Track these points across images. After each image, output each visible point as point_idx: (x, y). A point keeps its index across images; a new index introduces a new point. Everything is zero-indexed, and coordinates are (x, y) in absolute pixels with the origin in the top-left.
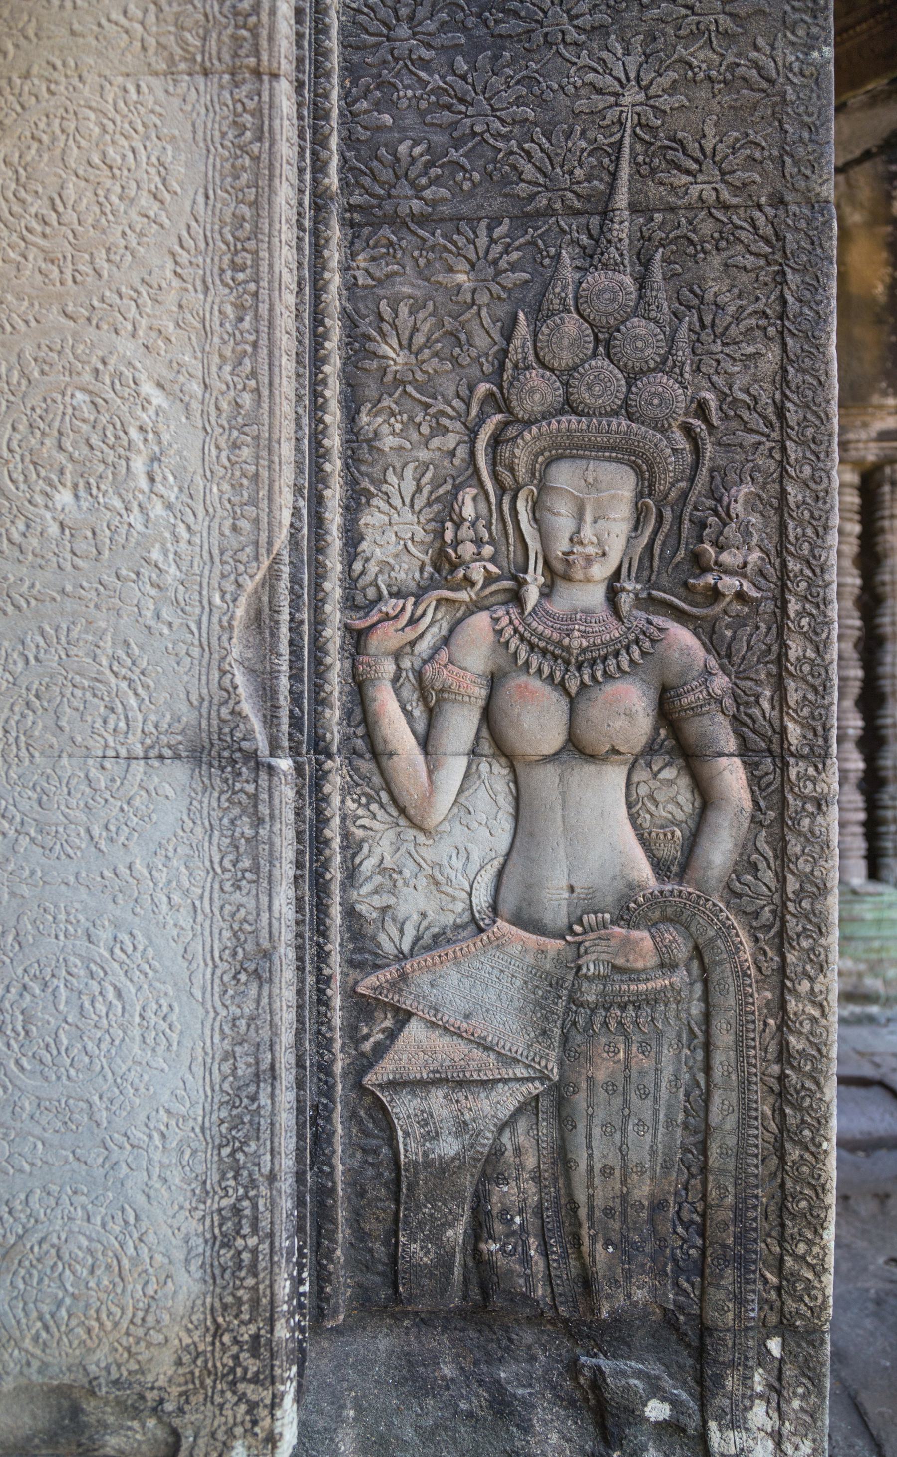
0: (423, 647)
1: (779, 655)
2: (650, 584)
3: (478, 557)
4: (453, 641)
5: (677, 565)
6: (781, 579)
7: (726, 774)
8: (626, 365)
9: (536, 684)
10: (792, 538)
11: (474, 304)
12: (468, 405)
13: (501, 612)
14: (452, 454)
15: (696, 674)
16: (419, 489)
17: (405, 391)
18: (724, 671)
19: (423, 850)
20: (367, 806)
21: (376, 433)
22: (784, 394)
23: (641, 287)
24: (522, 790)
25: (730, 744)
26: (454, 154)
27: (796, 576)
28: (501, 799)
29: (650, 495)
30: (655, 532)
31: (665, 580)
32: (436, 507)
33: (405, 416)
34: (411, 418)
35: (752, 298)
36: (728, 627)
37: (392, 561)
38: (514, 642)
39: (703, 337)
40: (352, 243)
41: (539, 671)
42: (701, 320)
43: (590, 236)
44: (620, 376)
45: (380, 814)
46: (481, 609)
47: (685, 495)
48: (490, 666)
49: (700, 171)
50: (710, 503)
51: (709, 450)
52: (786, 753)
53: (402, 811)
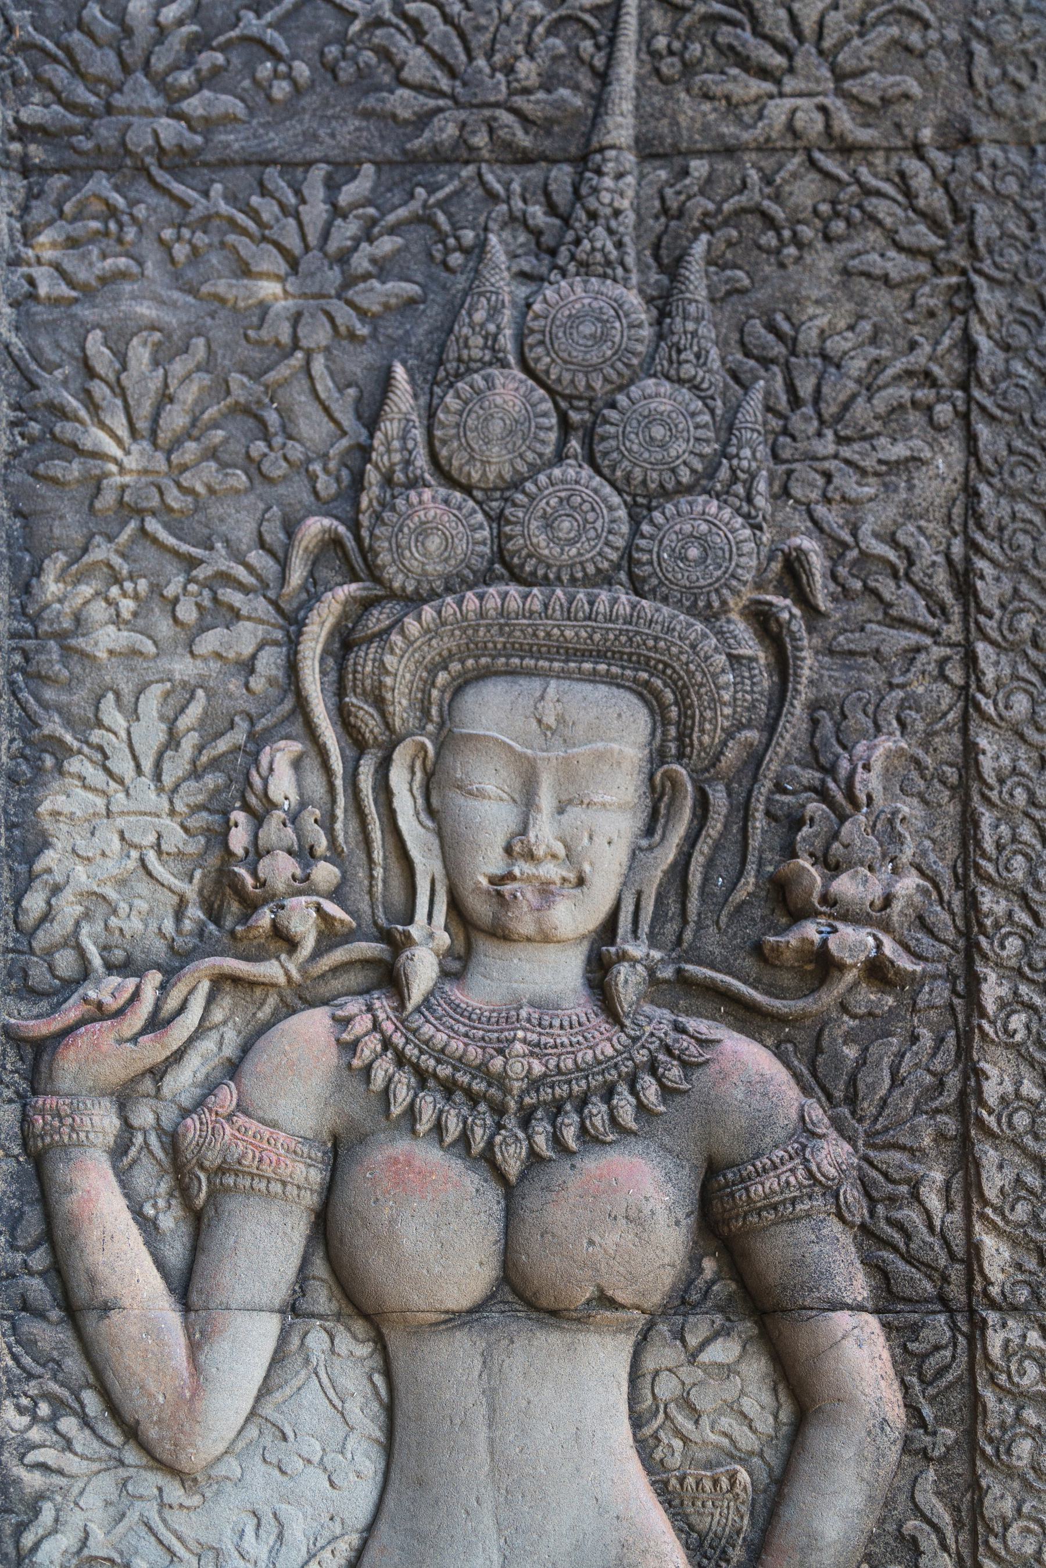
0: (183, 1081)
1: (963, 1095)
2: (679, 949)
3: (303, 884)
4: (247, 1067)
5: (739, 908)
6: (966, 934)
7: (849, 1346)
8: (628, 477)
9: (430, 1155)
10: (989, 846)
11: (296, 345)
12: (284, 564)
13: (353, 1006)
14: (248, 666)
15: (782, 1134)
16: (173, 741)
17: (143, 531)
18: (841, 1132)
19: (177, 1518)
20: (52, 1422)
21: (78, 619)
22: (971, 544)
23: (663, 314)
24: (401, 1388)
25: (859, 1286)
26: (252, 23)
27: (997, 926)
28: (354, 1409)
29: (680, 756)
30: (692, 839)
31: (712, 942)
32: (211, 780)
33: (143, 585)
34: (156, 589)
35: (902, 344)
36: (849, 1038)
37: (111, 894)
38: (383, 1068)
39: (796, 422)
40: (25, 209)
41: (439, 1128)
42: (791, 388)
43: (552, 209)
44: (616, 500)
45: (82, 1439)
46: (311, 1004)
47: (755, 760)
48: (330, 1120)
49: (791, 70)
50: (810, 776)
51: (808, 664)
52: (979, 1302)
53: (132, 1432)
